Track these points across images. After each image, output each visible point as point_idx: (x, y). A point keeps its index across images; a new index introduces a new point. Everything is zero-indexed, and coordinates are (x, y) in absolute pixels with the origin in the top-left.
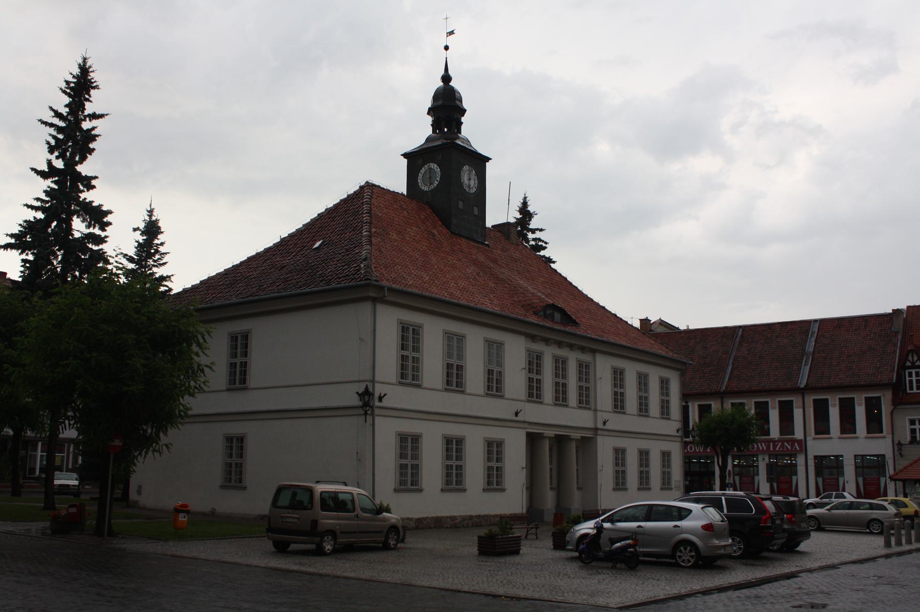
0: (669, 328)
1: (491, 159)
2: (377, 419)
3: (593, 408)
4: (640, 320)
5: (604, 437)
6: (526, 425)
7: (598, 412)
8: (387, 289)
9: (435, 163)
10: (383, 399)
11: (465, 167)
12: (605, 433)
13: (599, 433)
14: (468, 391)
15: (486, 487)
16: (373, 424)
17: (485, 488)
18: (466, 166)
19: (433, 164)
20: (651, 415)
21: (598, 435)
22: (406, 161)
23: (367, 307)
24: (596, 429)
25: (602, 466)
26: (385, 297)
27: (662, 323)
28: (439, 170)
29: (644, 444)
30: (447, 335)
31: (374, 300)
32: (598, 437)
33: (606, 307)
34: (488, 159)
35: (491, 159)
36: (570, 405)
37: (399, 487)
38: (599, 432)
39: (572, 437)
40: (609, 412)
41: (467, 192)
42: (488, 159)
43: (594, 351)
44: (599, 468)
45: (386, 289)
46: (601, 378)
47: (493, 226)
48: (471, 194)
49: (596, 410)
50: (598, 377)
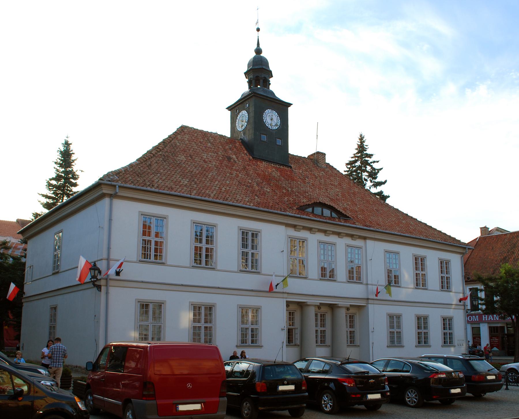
0: (501, 232)
1: (292, 104)
2: (112, 290)
3: (365, 282)
4: (480, 228)
5: (374, 305)
6: (285, 295)
7: (369, 286)
8: (119, 186)
9: (245, 110)
10: (120, 273)
11: (267, 111)
12: (376, 302)
13: (369, 303)
14: (219, 268)
15: (417, 344)
16: (107, 293)
17: (417, 345)
18: (269, 110)
19: (244, 111)
20: (429, 288)
21: (369, 304)
22: (229, 113)
23: (106, 201)
24: (368, 299)
25: (374, 328)
26: (117, 193)
27: (498, 229)
28: (247, 114)
29: (422, 311)
30: (195, 224)
31: (111, 196)
32: (369, 305)
33: (399, 209)
34: (290, 105)
35: (292, 104)
36: (339, 279)
37: (240, 344)
38: (370, 301)
39: (308, 304)
40: (97, 261)
41: (269, 128)
42: (290, 105)
43: (365, 238)
44: (370, 330)
45: (117, 186)
46: (371, 259)
47: (308, 156)
48: (275, 130)
49: (367, 284)
50: (368, 258)
